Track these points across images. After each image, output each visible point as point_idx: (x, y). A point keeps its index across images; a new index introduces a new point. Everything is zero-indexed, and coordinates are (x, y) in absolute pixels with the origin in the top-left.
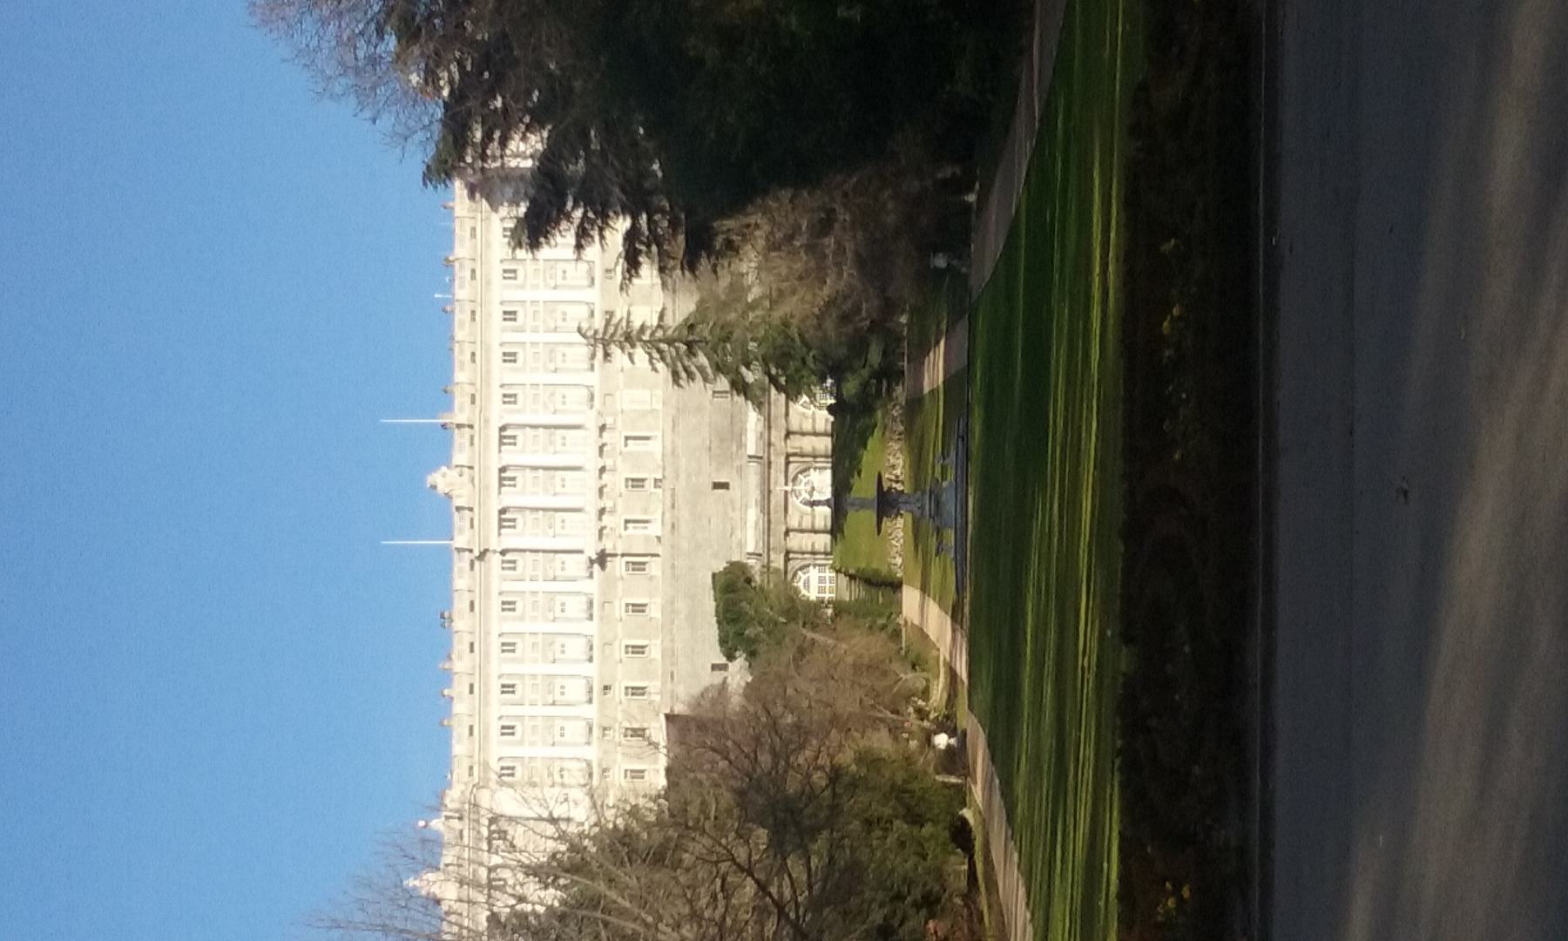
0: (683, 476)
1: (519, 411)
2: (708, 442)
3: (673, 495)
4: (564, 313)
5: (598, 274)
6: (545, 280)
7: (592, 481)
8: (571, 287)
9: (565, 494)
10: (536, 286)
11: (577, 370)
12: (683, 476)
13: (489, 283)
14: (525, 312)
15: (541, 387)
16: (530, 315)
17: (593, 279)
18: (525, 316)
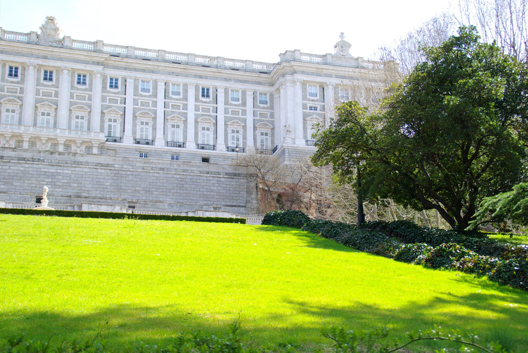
0: (53, 170)
1: (104, 88)
2: (85, 195)
3: (33, 160)
4: (178, 126)
5: (206, 153)
6: (202, 115)
7: (45, 133)
8: (196, 134)
9: (36, 115)
10: (197, 109)
11: (134, 132)
12: (53, 170)
13: (201, 77)
14: (180, 100)
15: (124, 105)
16: (177, 103)
17: (203, 148)
18: (176, 99)
